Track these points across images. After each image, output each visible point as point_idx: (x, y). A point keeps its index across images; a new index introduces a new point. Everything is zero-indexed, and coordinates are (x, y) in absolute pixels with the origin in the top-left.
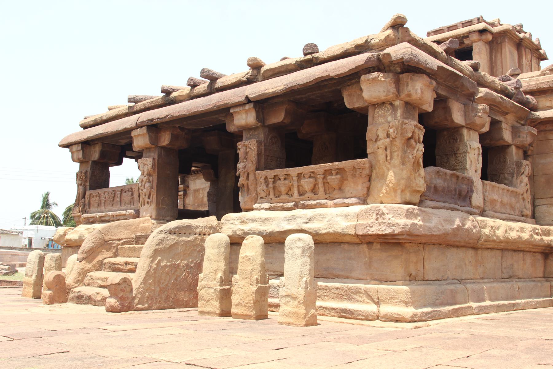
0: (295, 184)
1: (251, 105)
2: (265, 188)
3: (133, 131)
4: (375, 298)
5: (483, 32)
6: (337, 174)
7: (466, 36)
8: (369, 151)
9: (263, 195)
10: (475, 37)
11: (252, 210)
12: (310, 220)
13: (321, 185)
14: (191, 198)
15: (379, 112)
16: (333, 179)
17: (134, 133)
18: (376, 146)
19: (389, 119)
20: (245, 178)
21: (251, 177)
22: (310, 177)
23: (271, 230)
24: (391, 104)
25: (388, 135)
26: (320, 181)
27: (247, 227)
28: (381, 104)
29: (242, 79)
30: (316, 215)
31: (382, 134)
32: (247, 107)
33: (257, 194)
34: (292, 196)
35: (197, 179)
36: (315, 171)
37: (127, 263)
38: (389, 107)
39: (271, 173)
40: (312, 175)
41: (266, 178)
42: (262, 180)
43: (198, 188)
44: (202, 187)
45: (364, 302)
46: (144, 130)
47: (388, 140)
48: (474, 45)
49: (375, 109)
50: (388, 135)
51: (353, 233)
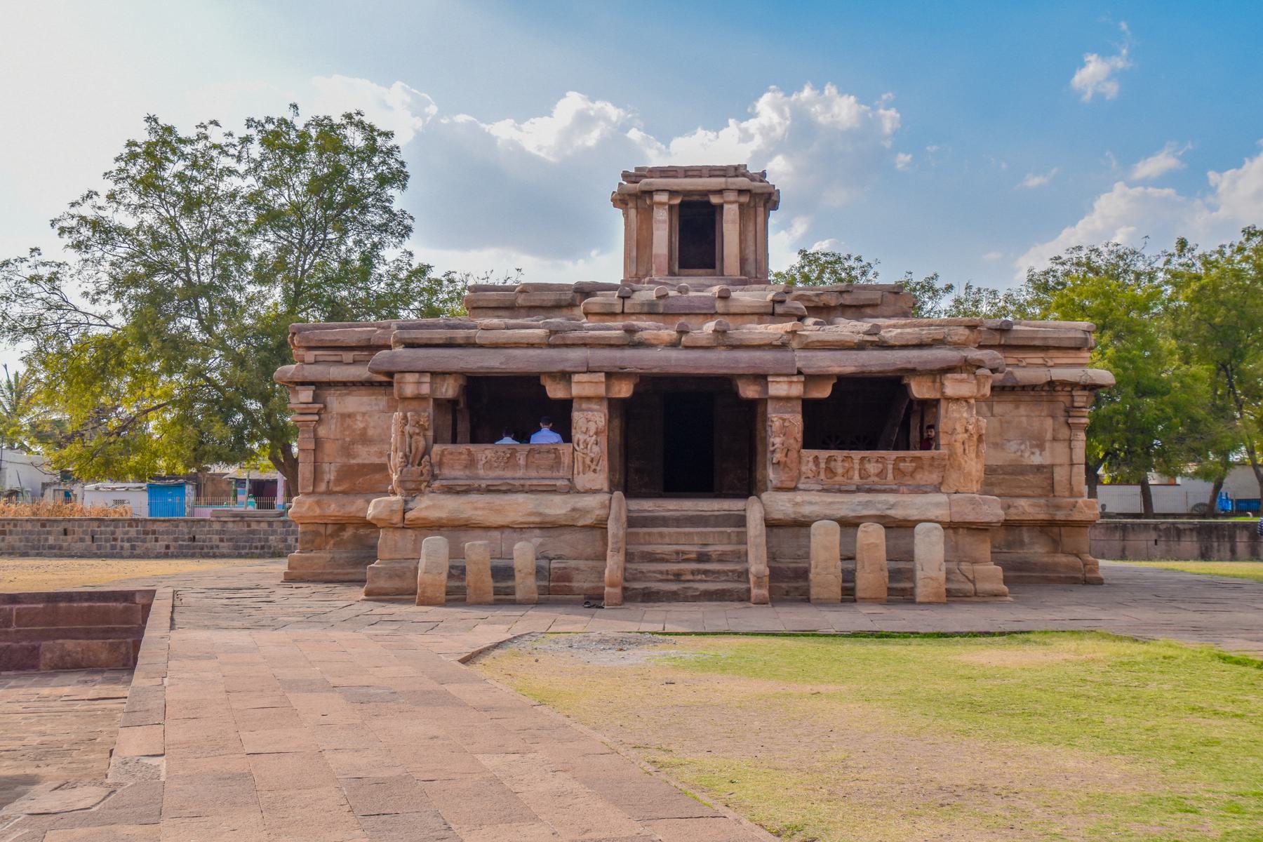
0: (857, 466)
1: (802, 379)
2: (814, 468)
3: (577, 375)
4: (971, 577)
5: (741, 192)
6: (911, 461)
7: (720, 192)
8: (942, 442)
9: (811, 475)
10: (732, 196)
11: (795, 489)
12: (892, 506)
13: (890, 471)
14: (333, 427)
15: (953, 407)
16: (907, 466)
17: (576, 378)
18: (953, 439)
19: (965, 415)
20: (784, 454)
21: (793, 455)
22: (877, 461)
23: (842, 514)
24: (966, 401)
25: (966, 431)
26: (890, 467)
27: (807, 510)
28: (957, 400)
29: (775, 343)
30: (899, 502)
31: (959, 428)
32: (795, 379)
33: (800, 473)
34: (851, 479)
35: (348, 394)
36: (886, 457)
37: (677, 553)
38: (964, 404)
39: (823, 454)
40: (880, 460)
41: (816, 457)
42: (811, 459)
43: (351, 410)
44: (363, 409)
45: (958, 581)
46: (601, 377)
47: (966, 435)
48: (726, 207)
49: (949, 403)
50: (966, 431)
51: (948, 520)
